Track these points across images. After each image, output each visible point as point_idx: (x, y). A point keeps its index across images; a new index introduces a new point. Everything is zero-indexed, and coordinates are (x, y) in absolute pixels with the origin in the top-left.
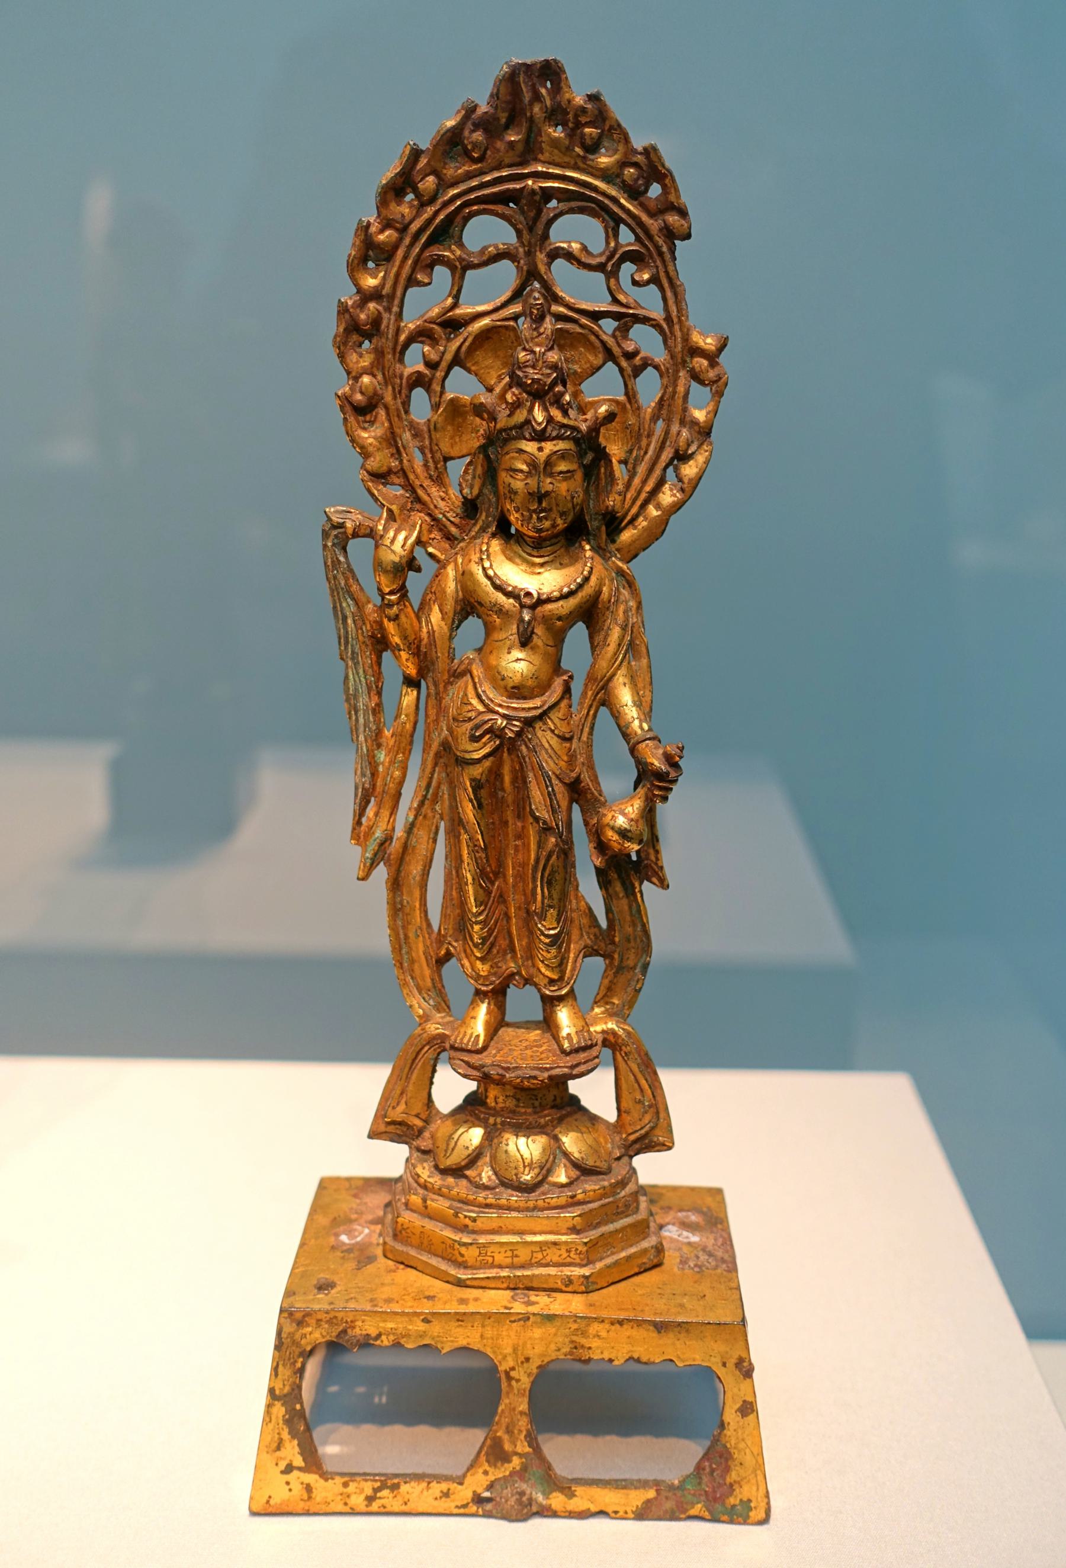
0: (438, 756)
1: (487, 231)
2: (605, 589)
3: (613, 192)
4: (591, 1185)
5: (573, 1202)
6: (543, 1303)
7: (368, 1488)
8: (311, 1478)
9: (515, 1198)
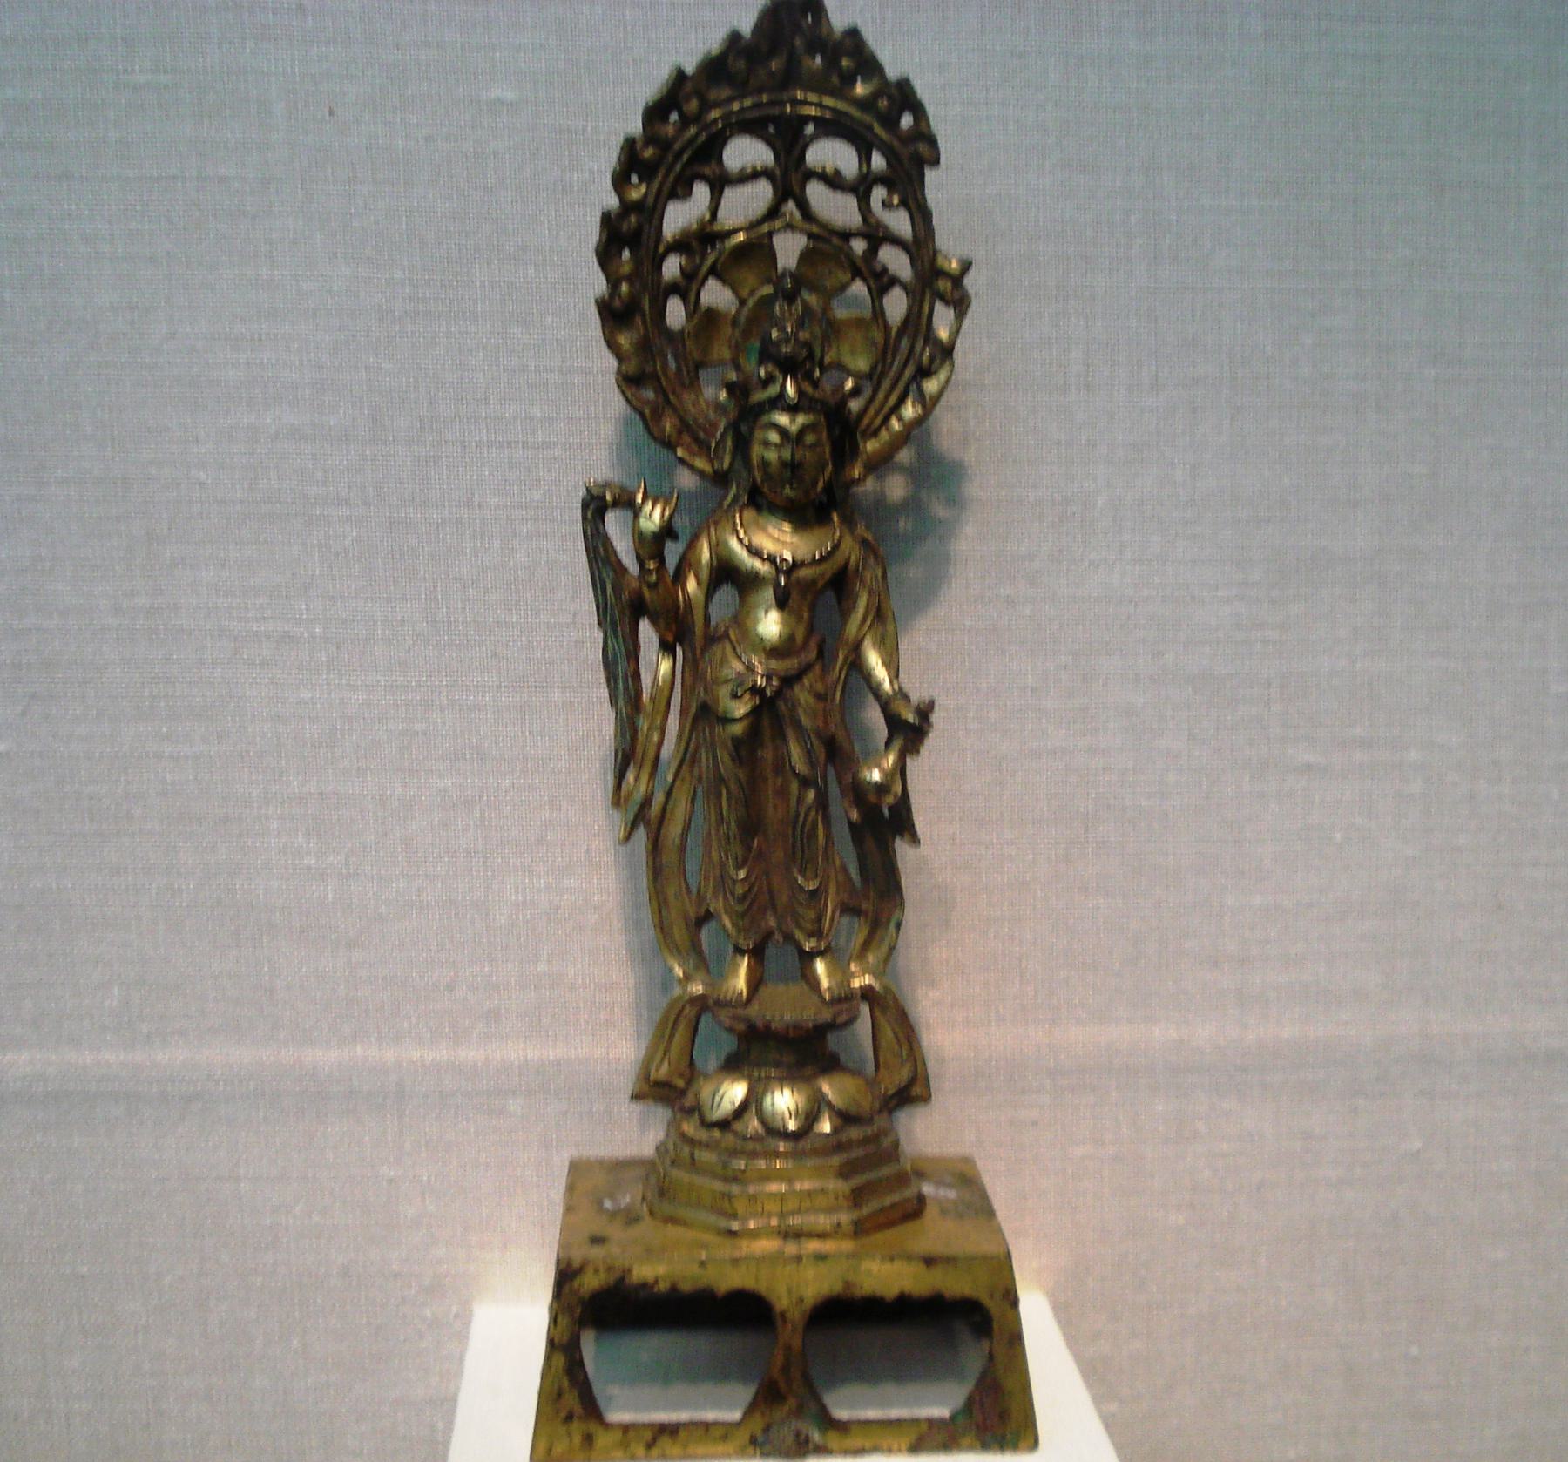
0: (695, 720)
1: (744, 152)
2: (853, 558)
3: (867, 118)
4: (854, 1133)
5: (839, 1147)
6: (813, 1246)
7: (648, 1435)
8: (593, 1427)
9: (782, 1147)
